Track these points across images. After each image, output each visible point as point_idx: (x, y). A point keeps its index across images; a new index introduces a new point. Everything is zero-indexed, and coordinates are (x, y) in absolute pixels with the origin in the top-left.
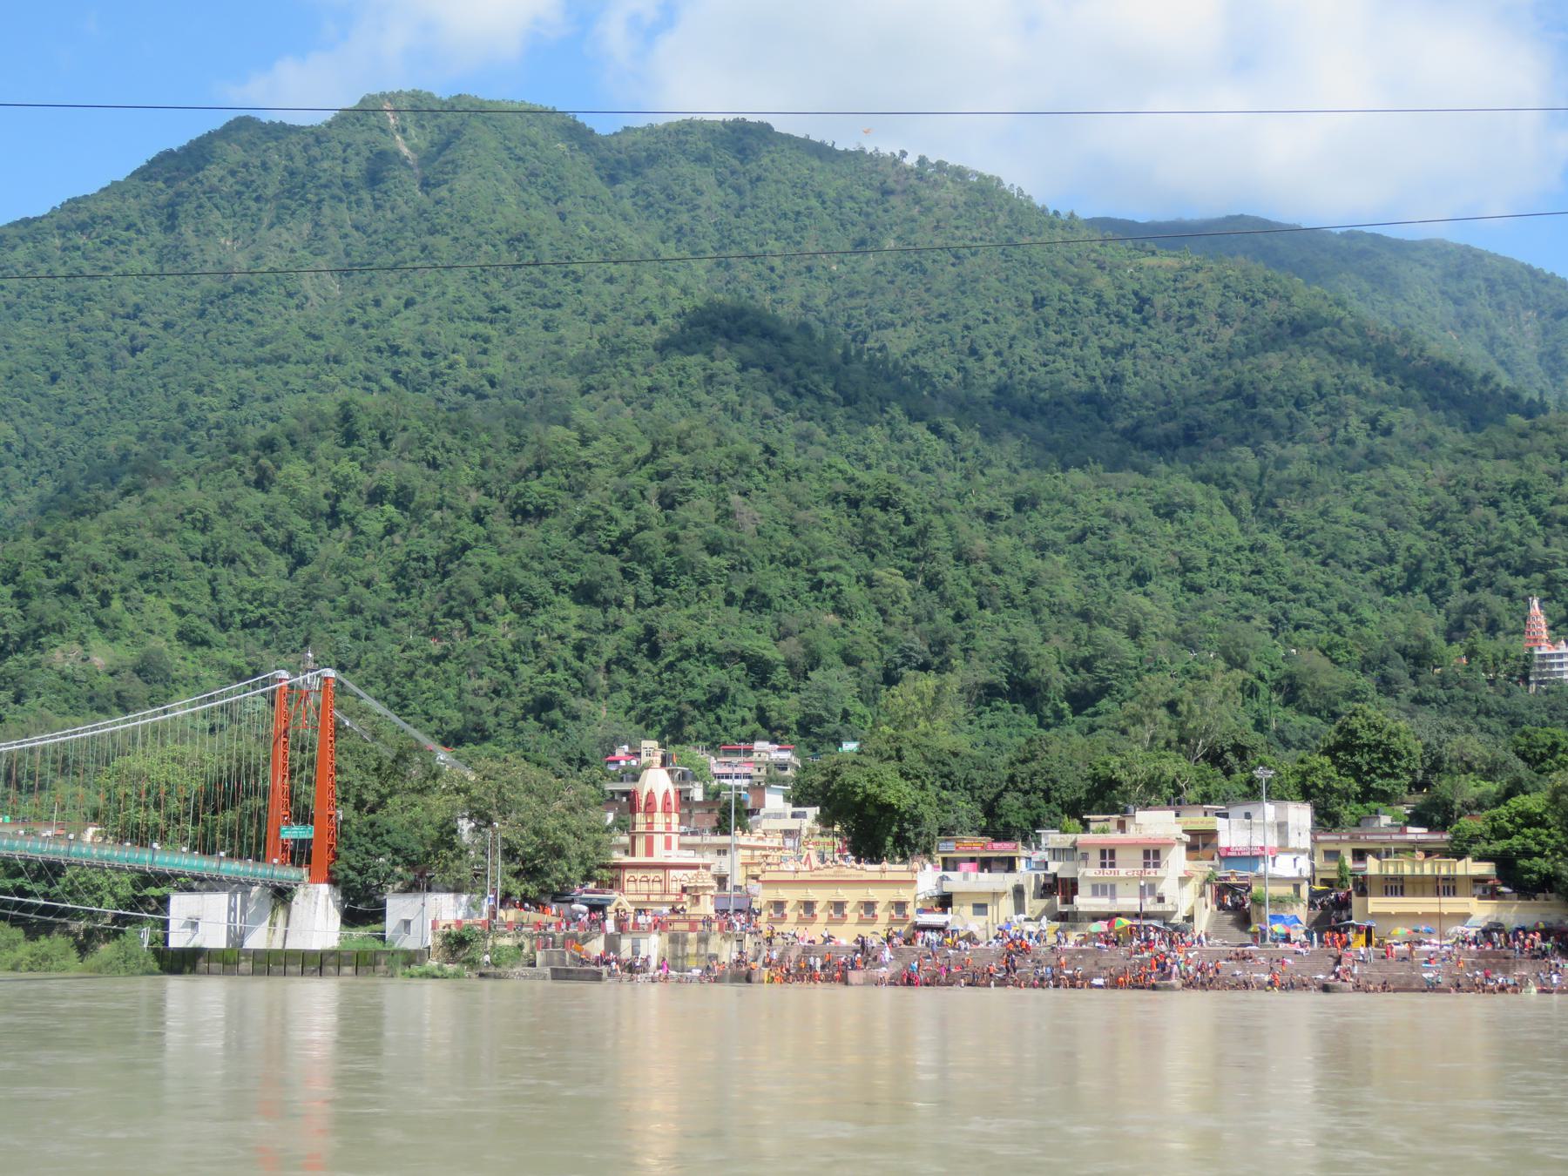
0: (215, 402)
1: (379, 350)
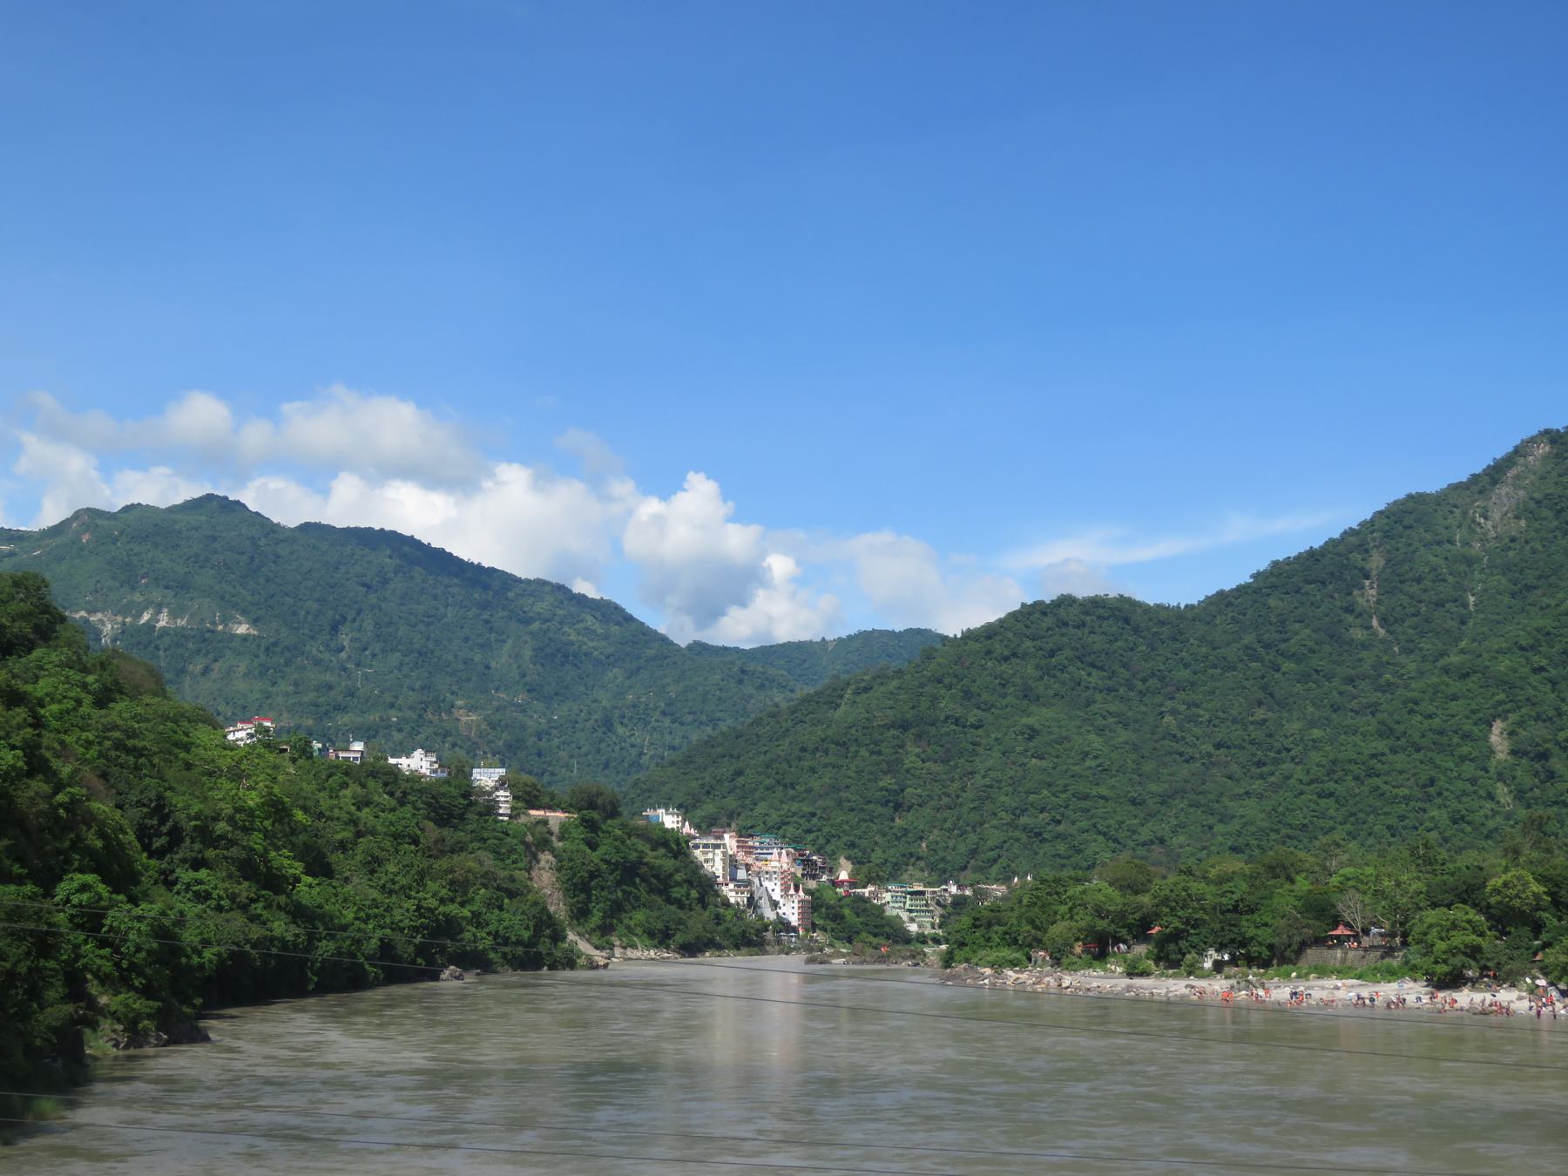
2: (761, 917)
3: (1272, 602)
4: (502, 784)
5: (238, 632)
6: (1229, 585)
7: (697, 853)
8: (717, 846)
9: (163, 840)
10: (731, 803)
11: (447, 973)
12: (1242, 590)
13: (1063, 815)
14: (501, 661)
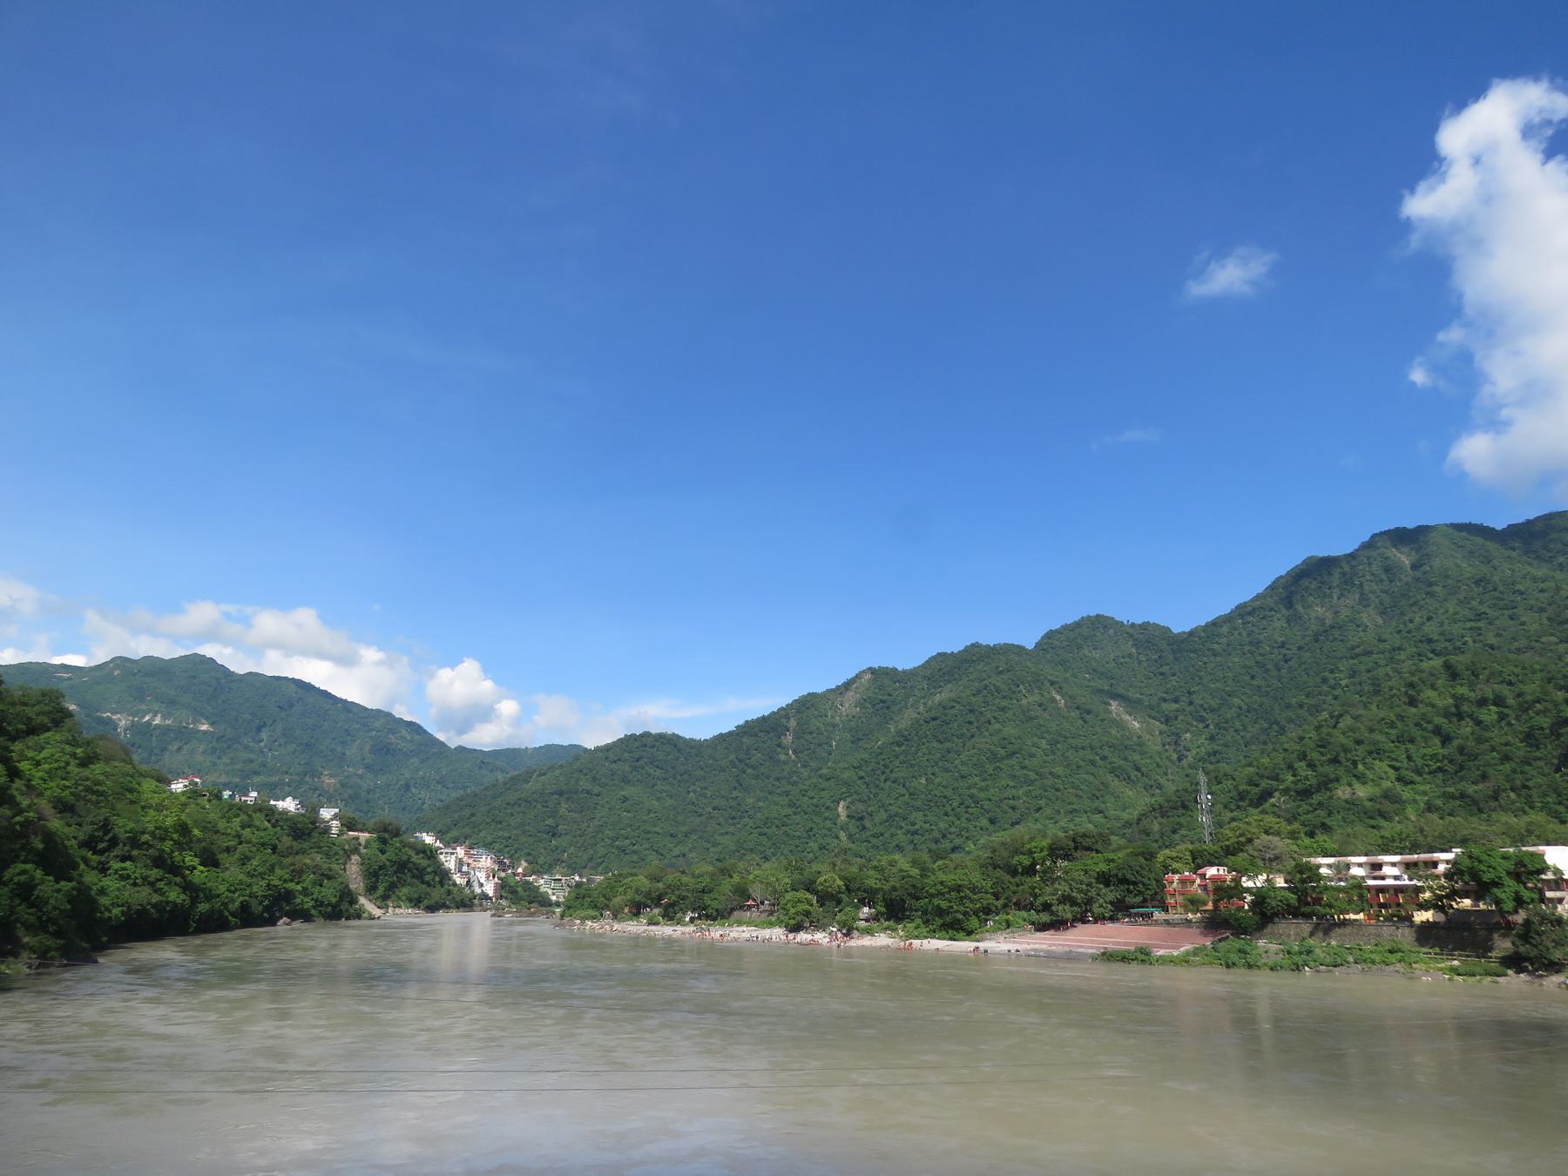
0: (1342, 676)
1: (1421, 641)
2: (473, 892)
3: (744, 740)
4: (335, 817)
6: (725, 731)
7: (442, 857)
8: (452, 854)
9: (104, 845)
10: (467, 830)
11: (281, 921)
12: (730, 733)
13: (637, 841)
14: (352, 751)
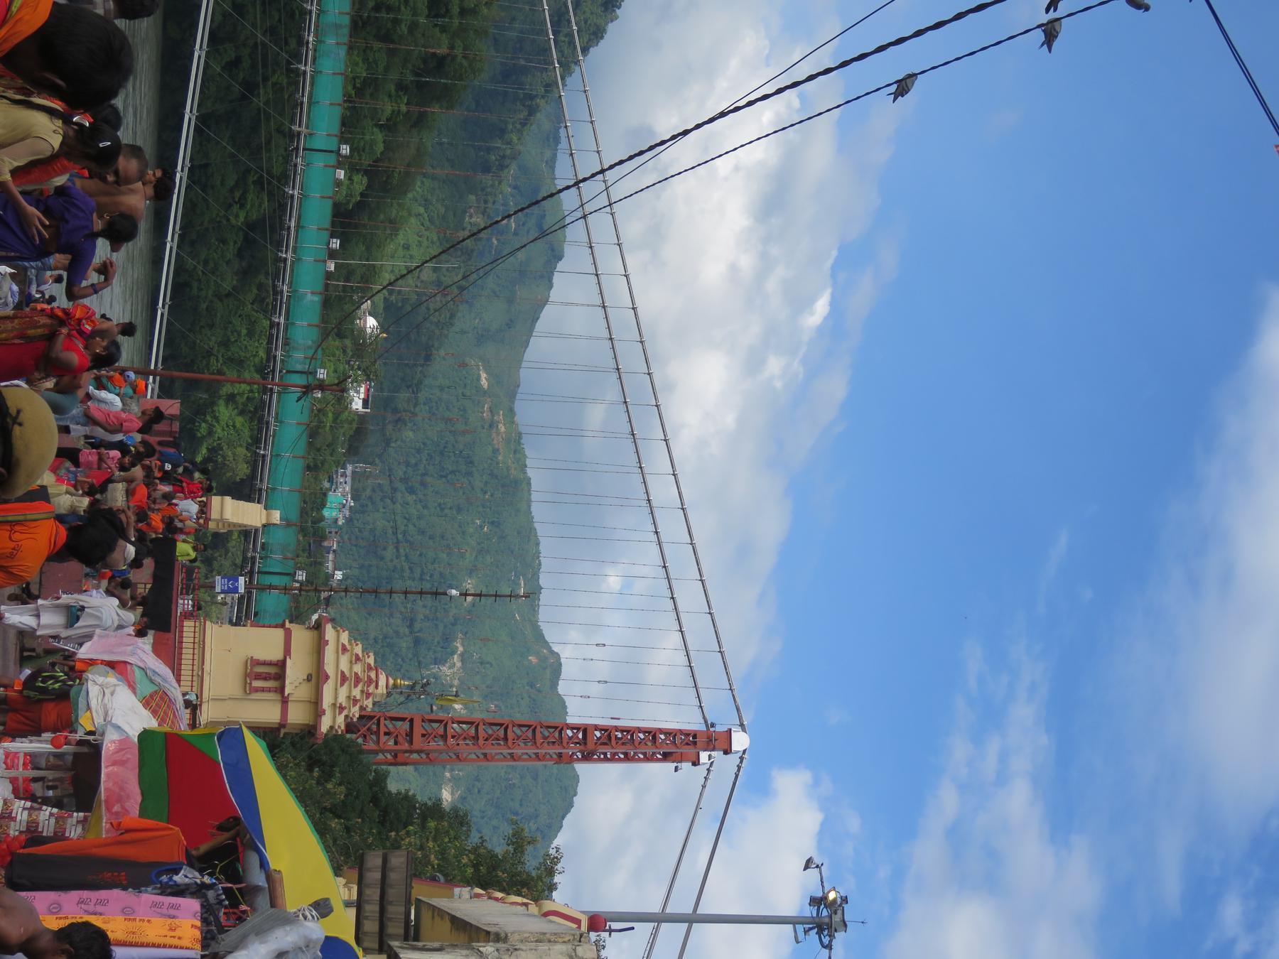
5: (443, 790)
